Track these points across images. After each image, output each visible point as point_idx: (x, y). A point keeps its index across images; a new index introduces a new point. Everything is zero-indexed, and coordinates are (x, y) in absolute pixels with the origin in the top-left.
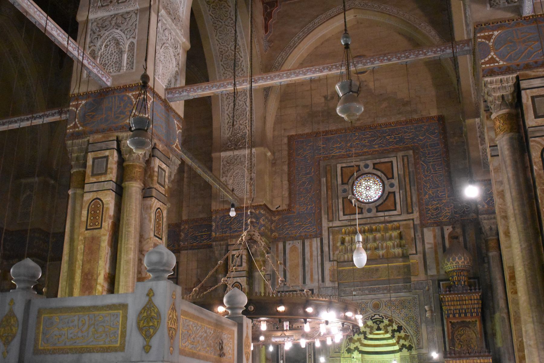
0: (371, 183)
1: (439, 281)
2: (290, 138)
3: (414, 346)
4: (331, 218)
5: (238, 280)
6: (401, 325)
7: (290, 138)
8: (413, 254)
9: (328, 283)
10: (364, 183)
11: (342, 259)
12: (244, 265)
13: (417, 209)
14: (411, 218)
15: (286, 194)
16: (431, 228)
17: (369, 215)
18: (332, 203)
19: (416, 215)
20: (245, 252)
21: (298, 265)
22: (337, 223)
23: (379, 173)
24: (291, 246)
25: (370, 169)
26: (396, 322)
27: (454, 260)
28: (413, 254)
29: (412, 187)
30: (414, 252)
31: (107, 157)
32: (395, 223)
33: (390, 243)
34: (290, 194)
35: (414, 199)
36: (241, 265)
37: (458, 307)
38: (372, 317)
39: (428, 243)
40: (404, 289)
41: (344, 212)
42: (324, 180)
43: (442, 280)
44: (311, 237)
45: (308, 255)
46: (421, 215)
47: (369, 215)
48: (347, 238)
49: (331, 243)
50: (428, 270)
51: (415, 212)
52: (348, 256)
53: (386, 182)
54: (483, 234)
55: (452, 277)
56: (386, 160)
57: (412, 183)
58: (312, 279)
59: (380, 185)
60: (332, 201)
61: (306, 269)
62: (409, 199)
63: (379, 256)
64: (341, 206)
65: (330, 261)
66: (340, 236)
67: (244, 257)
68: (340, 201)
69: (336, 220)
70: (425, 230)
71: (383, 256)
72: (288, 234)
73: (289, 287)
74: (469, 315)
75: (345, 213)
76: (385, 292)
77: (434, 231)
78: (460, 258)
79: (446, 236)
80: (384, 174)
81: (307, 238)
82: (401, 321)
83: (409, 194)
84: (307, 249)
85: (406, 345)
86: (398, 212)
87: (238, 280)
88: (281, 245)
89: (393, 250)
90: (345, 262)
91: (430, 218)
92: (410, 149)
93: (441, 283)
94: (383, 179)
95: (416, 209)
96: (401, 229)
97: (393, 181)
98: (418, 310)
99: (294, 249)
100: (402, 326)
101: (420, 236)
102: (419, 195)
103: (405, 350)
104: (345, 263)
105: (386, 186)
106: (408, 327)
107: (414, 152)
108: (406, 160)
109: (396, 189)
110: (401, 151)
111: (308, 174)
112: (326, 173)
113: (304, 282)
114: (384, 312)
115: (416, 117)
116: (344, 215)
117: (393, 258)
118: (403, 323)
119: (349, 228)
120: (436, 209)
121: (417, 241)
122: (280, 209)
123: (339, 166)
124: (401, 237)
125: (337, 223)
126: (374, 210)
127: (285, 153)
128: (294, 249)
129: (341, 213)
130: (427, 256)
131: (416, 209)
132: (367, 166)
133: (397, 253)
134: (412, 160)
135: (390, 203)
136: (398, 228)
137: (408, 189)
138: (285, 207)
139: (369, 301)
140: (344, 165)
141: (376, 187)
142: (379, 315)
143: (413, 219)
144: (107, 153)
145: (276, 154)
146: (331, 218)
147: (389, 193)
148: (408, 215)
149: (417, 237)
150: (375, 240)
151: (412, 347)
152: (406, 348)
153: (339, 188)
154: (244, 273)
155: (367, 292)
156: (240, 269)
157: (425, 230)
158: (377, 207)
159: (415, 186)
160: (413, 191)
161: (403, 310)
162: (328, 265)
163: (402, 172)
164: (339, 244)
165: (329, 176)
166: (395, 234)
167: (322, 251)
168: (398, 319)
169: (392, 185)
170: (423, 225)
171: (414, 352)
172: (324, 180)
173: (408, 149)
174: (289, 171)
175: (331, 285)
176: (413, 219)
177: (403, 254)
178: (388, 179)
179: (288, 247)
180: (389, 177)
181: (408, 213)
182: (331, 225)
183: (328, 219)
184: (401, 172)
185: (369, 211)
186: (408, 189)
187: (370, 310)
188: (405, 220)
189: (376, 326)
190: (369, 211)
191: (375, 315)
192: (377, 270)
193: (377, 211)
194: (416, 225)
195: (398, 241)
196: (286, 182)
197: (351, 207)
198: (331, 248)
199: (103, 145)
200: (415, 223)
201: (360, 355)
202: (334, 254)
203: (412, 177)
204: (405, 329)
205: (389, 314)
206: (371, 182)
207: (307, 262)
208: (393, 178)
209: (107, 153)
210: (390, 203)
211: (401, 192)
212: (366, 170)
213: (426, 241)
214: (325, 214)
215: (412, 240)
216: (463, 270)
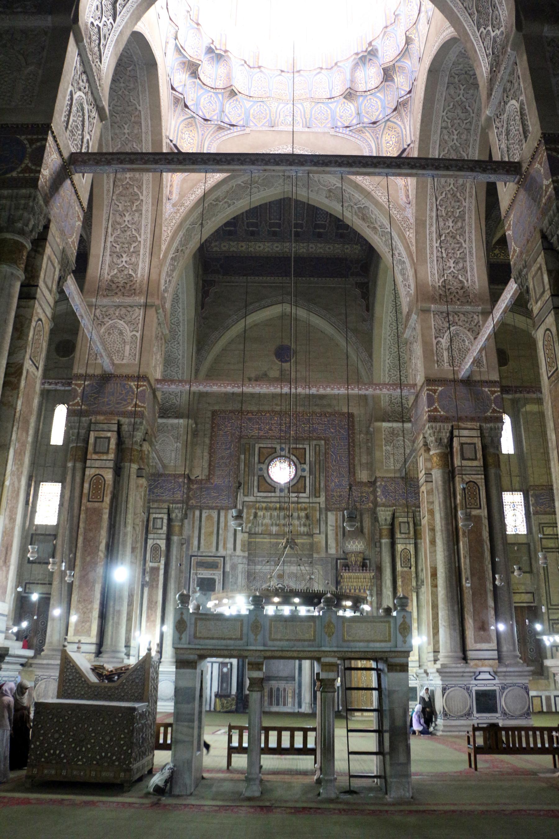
1: (337, 559)
2: (214, 413)
4: (246, 493)
5: (158, 542)
7: (214, 413)
9: (239, 552)
11: (253, 531)
12: (165, 528)
15: (206, 465)
16: (335, 513)
19: (322, 499)
20: (165, 517)
21: (212, 533)
22: (252, 499)
24: (207, 514)
27: (354, 543)
30: (318, 532)
31: (109, 438)
34: (210, 465)
35: (322, 485)
36: (162, 528)
37: (355, 584)
39: (331, 526)
41: (258, 489)
42: (242, 457)
43: (339, 559)
44: (227, 509)
45: (222, 525)
48: (260, 513)
53: (299, 466)
54: (378, 521)
55: (350, 558)
56: (301, 446)
58: (225, 547)
61: (220, 537)
62: (317, 484)
65: (242, 532)
66: (254, 511)
67: (165, 521)
68: (256, 478)
70: (329, 514)
72: (204, 503)
73: (202, 552)
74: (362, 591)
77: (336, 515)
78: (359, 543)
80: (297, 458)
81: (223, 509)
84: (222, 519)
87: (158, 542)
88: (197, 513)
90: (256, 534)
91: (334, 504)
92: (322, 439)
95: (323, 494)
97: (304, 466)
99: (209, 517)
102: (326, 481)
107: (325, 443)
108: (318, 449)
109: (306, 474)
110: (315, 440)
111: (227, 449)
112: (245, 450)
113: (217, 549)
116: (259, 491)
121: (322, 523)
122: (200, 478)
124: (307, 517)
125: (252, 499)
127: (208, 426)
128: (209, 517)
130: (329, 537)
131: (323, 494)
132: (282, 449)
133: (302, 531)
134: (323, 449)
135: (300, 485)
137: (317, 476)
138: (204, 478)
140: (262, 446)
143: (319, 503)
144: (109, 434)
145: (199, 426)
146: (246, 493)
153: (256, 466)
154: (164, 536)
156: (160, 531)
157: (329, 514)
160: (322, 478)
164: (252, 518)
165: (247, 453)
169: (303, 470)
170: (327, 509)
172: (242, 457)
173: (320, 439)
174: (211, 443)
175: (242, 554)
178: (301, 463)
179: (204, 515)
182: (246, 499)
184: (313, 459)
185: (281, 490)
186: (317, 476)
195: (303, 520)
196: (206, 454)
197: (267, 485)
199: (105, 427)
202: (246, 527)
207: (221, 532)
208: (305, 463)
209: (109, 434)
210: (300, 485)
212: (283, 453)
213: (329, 523)
216: (360, 553)
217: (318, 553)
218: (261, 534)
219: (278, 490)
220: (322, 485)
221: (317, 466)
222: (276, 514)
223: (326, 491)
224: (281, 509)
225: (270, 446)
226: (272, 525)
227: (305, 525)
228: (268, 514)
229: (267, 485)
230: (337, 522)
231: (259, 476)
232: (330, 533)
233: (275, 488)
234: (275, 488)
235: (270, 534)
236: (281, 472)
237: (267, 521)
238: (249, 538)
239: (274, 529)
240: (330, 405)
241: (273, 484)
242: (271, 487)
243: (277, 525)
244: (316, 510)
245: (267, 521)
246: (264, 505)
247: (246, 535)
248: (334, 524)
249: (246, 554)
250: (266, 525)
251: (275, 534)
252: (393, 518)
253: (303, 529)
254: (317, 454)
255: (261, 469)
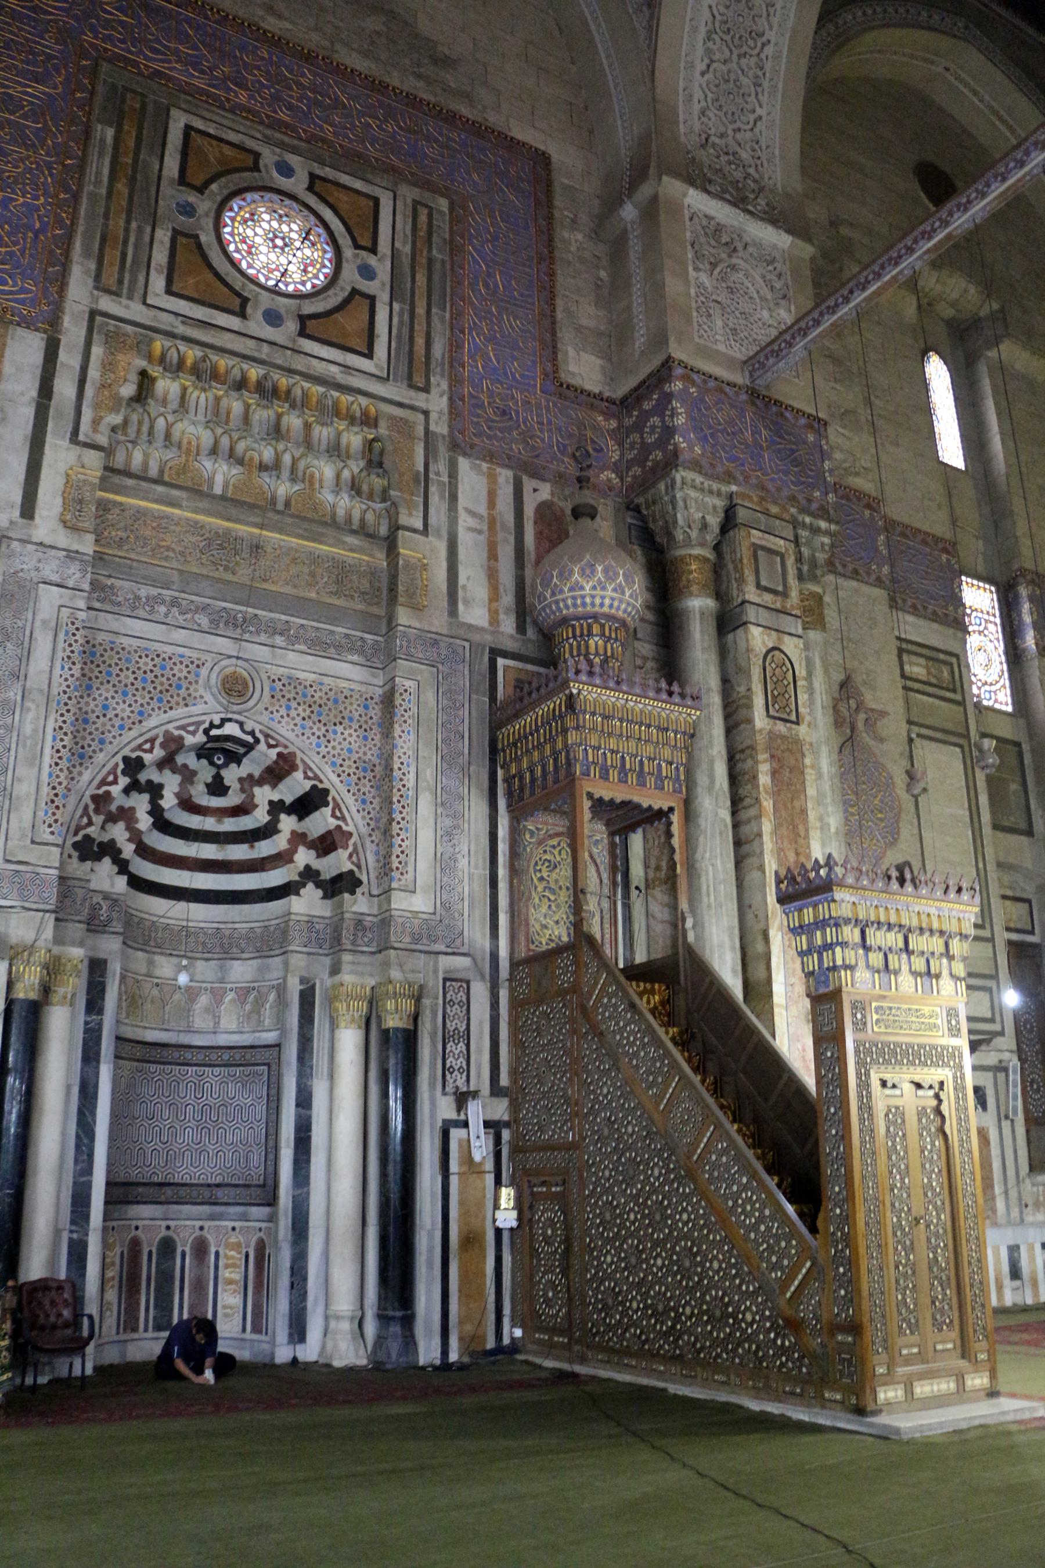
0: (293, 229)
1: (495, 653)
3: (364, 878)
6: (326, 785)
8: (415, 531)
9: (47, 524)
10: (267, 221)
11: (119, 460)
13: (445, 385)
14: (423, 405)
16: (485, 466)
17: (268, 332)
18: (127, 230)
19: (437, 402)
22: (134, 310)
23: (328, 215)
25: (298, 184)
26: (307, 767)
28: (415, 531)
29: (434, 310)
30: (419, 524)
32: (364, 401)
33: (327, 470)
35: (439, 349)
38: (212, 726)
39: (469, 512)
40: (351, 650)
41: (169, 281)
43: (505, 654)
46: (454, 412)
47: (268, 332)
48: (167, 386)
49: (94, 373)
50: (461, 607)
51: (434, 391)
52: (146, 456)
53: (348, 252)
57: (435, 297)
59: (325, 252)
60: (128, 222)
62: (420, 341)
63: (273, 501)
64: (160, 256)
68: (163, 236)
69: (130, 297)
71: (287, 504)
75: (174, 289)
76: (279, 640)
77: (492, 478)
79: (529, 511)
82: (328, 770)
83: (420, 326)
85: (317, 873)
86: (376, 366)
89: (328, 497)
93: (501, 662)
94: (341, 241)
96: (383, 430)
98: (412, 737)
100: (326, 792)
101: (445, 479)
103: (311, 892)
104: (130, 482)
105: (345, 265)
106: (350, 800)
108: (423, 218)
109: (379, 287)
114: (265, 717)
115: (465, 111)
116: (169, 292)
117: (325, 524)
118: (331, 780)
119: (183, 347)
120: (504, 413)
121: (433, 489)
123: (178, 122)
125: (134, 310)
126: (291, 326)
129: (158, 282)
131: (440, 384)
132: (286, 170)
133: (341, 512)
134: (443, 224)
136: (368, 421)
137: (421, 310)
139: (208, 657)
141: (308, 252)
142: (241, 725)
143: (426, 413)
147: (354, 292)
148: (412, 393)
149: (432, 476)
150: (276, 432)
151: (359, 883)
152: (319, 884)
155: (204, 621)
158: (303, 319)
159: (444, 309)
160: (436, 322)
161: (339, 729)
162: (60, 458)
163: (408, 249)
166: (354, 439)
167: (46, 389)
168: (317, 759)
169: (367, 273)
171: (359, 904)
175: (63, 539)
176: (426, 413)
177: (362, 520)
180: (363, 243)
181: (412, 386)
182: (106, 303)
183: (98, 277)
186: (421, 310)
187: (208, 697)
188: (400, 405)
189: (205, 773)
190: (273, 318)
191: (224, 721)
192: (257, 548)
193: (303, 333)
194: (434, 433)
195: (356, 466)
198: (89, 391)
200: (432, 427)
201: (121, 884)
202: (96, 422)
203: (436, 278)
204: (337, 806)
205: (285, 731)
206: (294, 227)
208: (373, 250)
210: (353, 322)
211: (396, 306)
212: (284, 183)
213: (462, 502)
214: (87, 253)
215: (417, 481)
217: (417, 609)
218: (155, 481)
219: (256, 314)
220: (439, 349)
221: (421, 279)
222: (237, 407)
223: (455, 382)
224: (268, 392)
225: (233, 137)
226: (214, 451)
227: (355, 488)
228: (200, 398)
229: (210, 276)
230: (492, 503)
231: (176, 233)
232: (466, 540)
233: (245, 301)
234: (245, 301)
235: (199, 492)
236: (275, 248)
237: (194, 430)
238: (104, 484)
239: (221, 474)
240: (469, 98)
241: (237, 282)
242: (232, 293)
243: (232, 456)
244: (411, 437)
245: (194, 430)
246: (192, 354)
247: (94, 459)
248: (482, 509)
249: (87, 545)
250: (191, 451)
251: (223, 498)
252: (729, 522)
253: (344, 504)
254: (422, 236)
255: (188, 210)
